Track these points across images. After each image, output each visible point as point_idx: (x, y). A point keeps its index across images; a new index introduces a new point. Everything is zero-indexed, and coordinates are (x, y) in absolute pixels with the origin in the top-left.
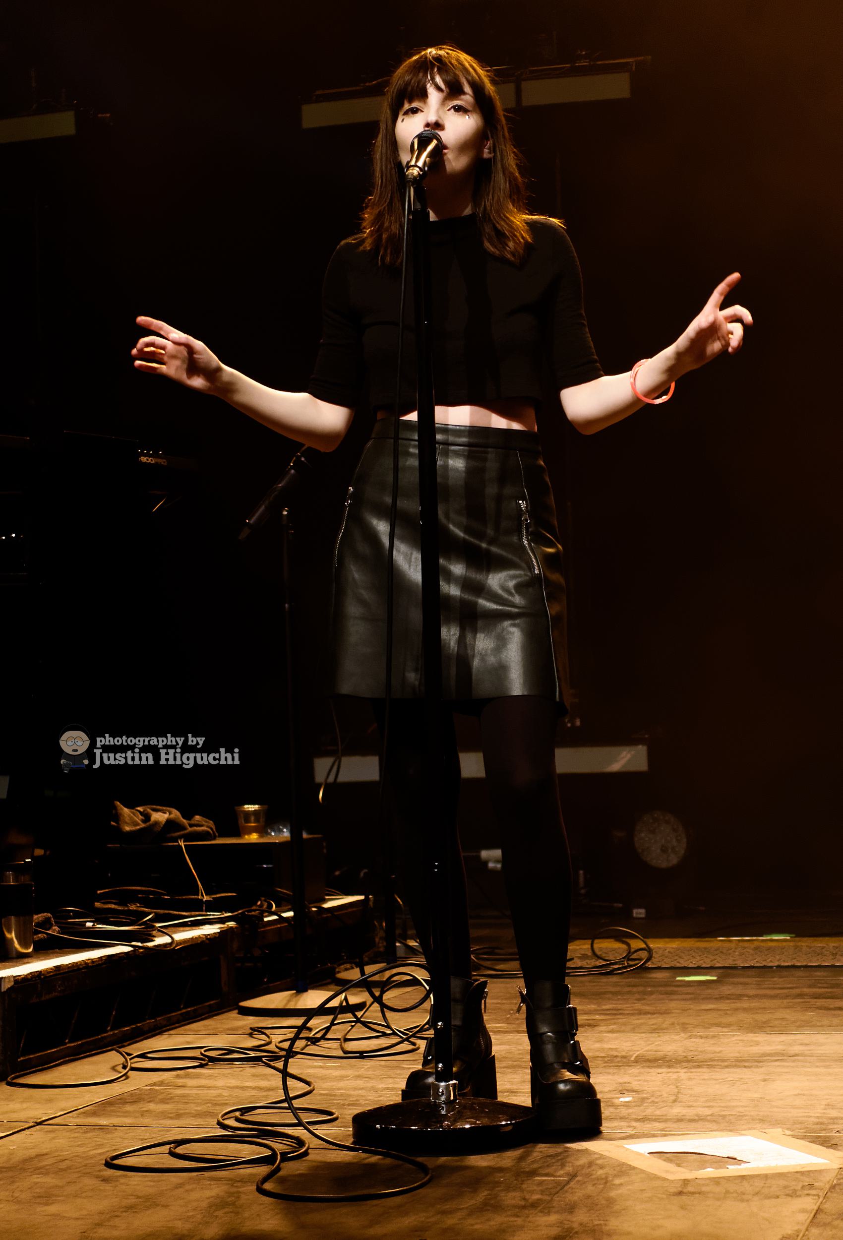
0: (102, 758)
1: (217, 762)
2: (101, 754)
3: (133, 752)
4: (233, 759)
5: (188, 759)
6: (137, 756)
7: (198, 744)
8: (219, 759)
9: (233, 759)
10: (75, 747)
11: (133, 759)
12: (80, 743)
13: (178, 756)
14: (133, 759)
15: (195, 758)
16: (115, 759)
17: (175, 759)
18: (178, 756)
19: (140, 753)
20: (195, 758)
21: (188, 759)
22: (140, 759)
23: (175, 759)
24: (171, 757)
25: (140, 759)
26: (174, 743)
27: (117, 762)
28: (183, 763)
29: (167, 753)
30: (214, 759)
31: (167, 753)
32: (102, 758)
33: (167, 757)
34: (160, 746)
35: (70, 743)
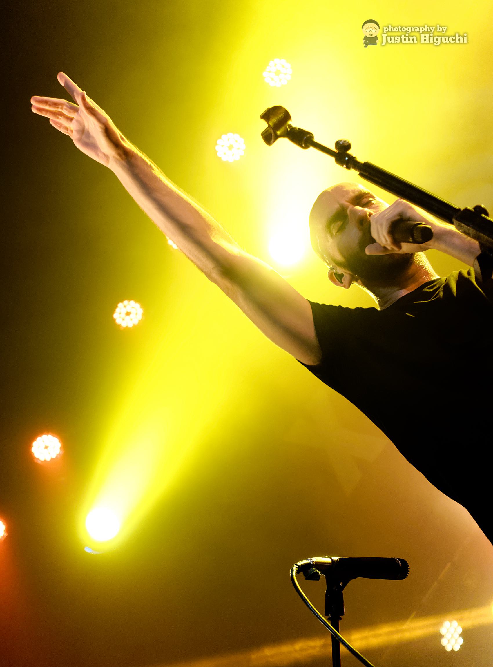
0: (387, 39)
1: (454, 41)
2: (386, 37)
3: (405, 36)
4: (463, 40)
5: (437, 40)
6: (407, 38)
7: (443, 31)
8: (455, 40)
9: (463, 40)
10: (371, 33)
11: (405, 40)
12: (374, 30)
13: (431, 38)
14: (405, 40)
15: (441, 39)
16: (394, 40)
17: (429, 40)
18: (431, 38)
19: (409, 36)
20: (441, 39)
21: (437, 40)
22: (409, 40)
23: (429, 40)
24: (427, 38)
25: (409, 40)
26: (429, 30)
27: (396, 42)
28: (434, 42)
29: (425, 37)
30: (452, 40)
31: (425, 37)
32: (387, 39)
33: (425, 38)
34: (421, 32)
35: (368, 31)
